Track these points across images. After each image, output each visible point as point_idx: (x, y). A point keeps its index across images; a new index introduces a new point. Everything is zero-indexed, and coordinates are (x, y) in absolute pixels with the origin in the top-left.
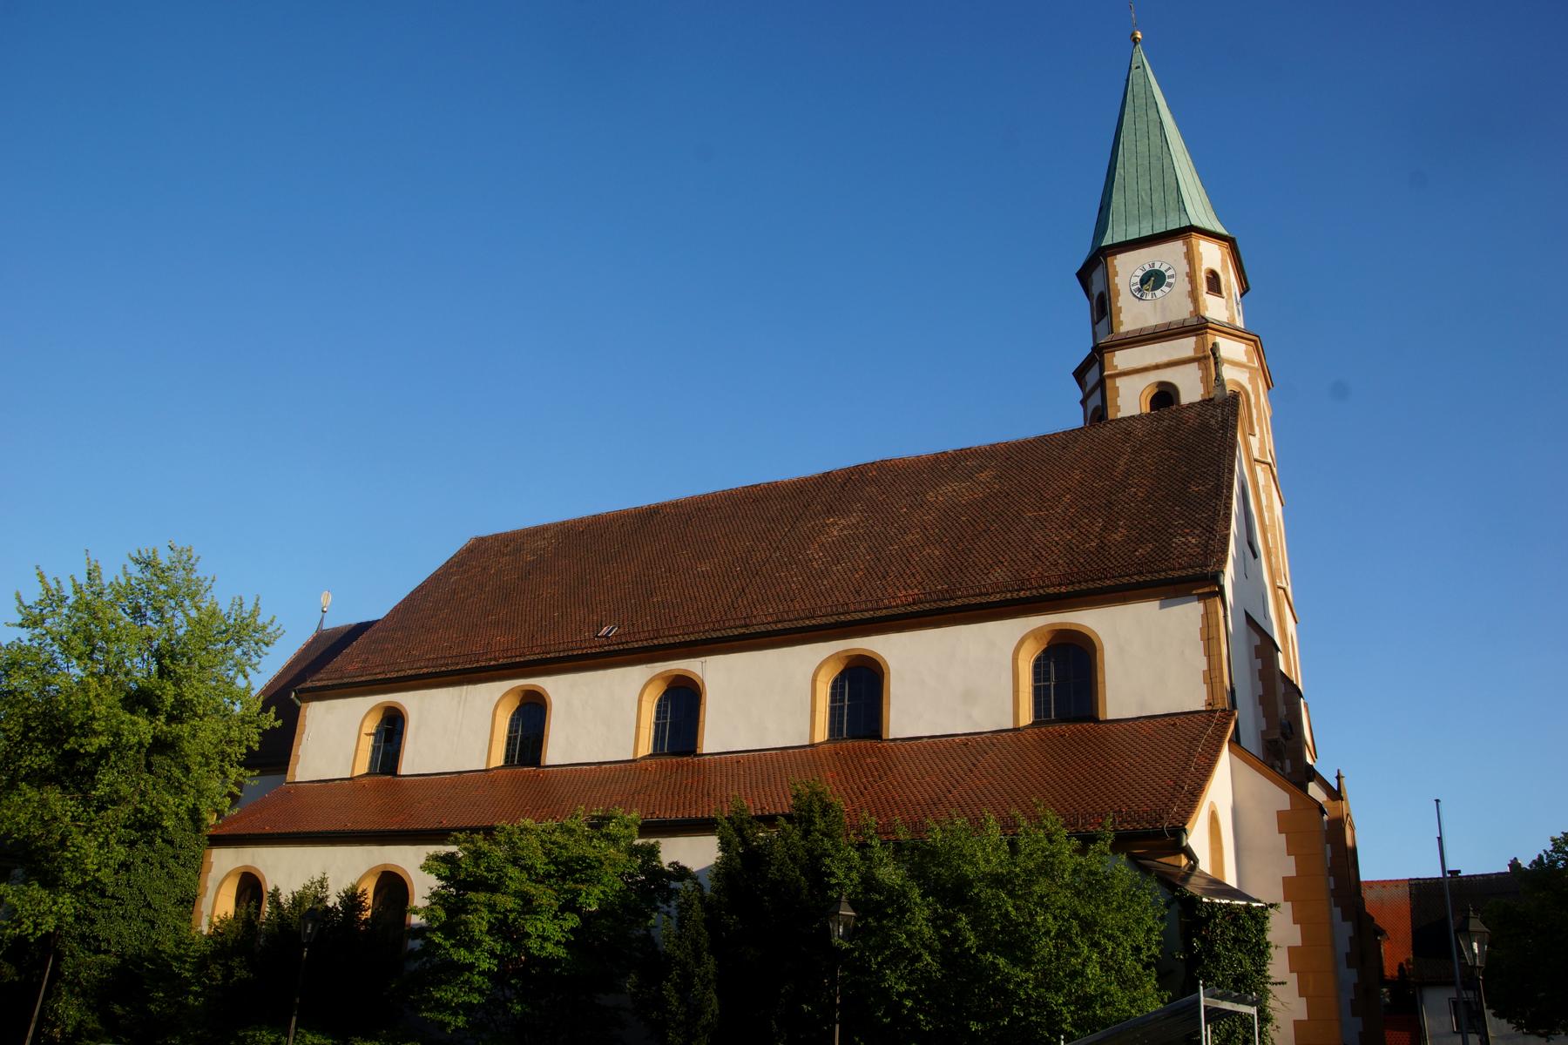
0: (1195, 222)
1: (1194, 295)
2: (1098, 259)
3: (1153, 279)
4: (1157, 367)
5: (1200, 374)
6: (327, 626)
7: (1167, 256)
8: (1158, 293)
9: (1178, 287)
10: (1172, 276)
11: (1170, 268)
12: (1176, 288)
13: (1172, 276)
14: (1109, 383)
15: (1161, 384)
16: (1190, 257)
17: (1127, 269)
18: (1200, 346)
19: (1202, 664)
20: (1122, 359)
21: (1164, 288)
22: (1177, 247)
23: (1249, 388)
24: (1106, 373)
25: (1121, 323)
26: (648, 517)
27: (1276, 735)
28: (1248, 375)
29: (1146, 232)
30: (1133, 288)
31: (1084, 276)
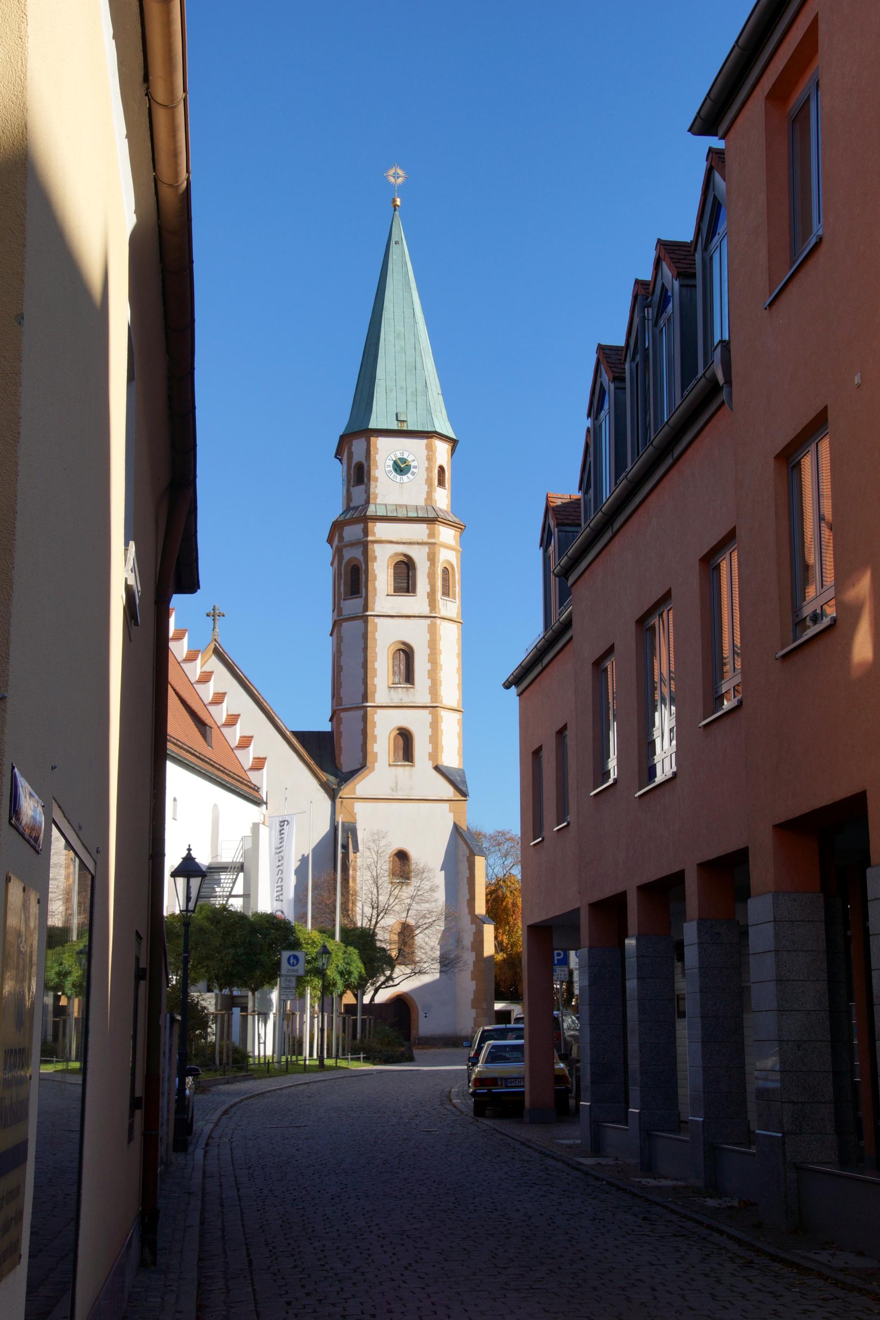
0: (439, 430)
8: (405, 477)
10: (415, 467)
11: (414, 460)
13: (415, 467)
21: (409, 475)
22: (420, 444)
30: (387, 469)
31: (345, 440)
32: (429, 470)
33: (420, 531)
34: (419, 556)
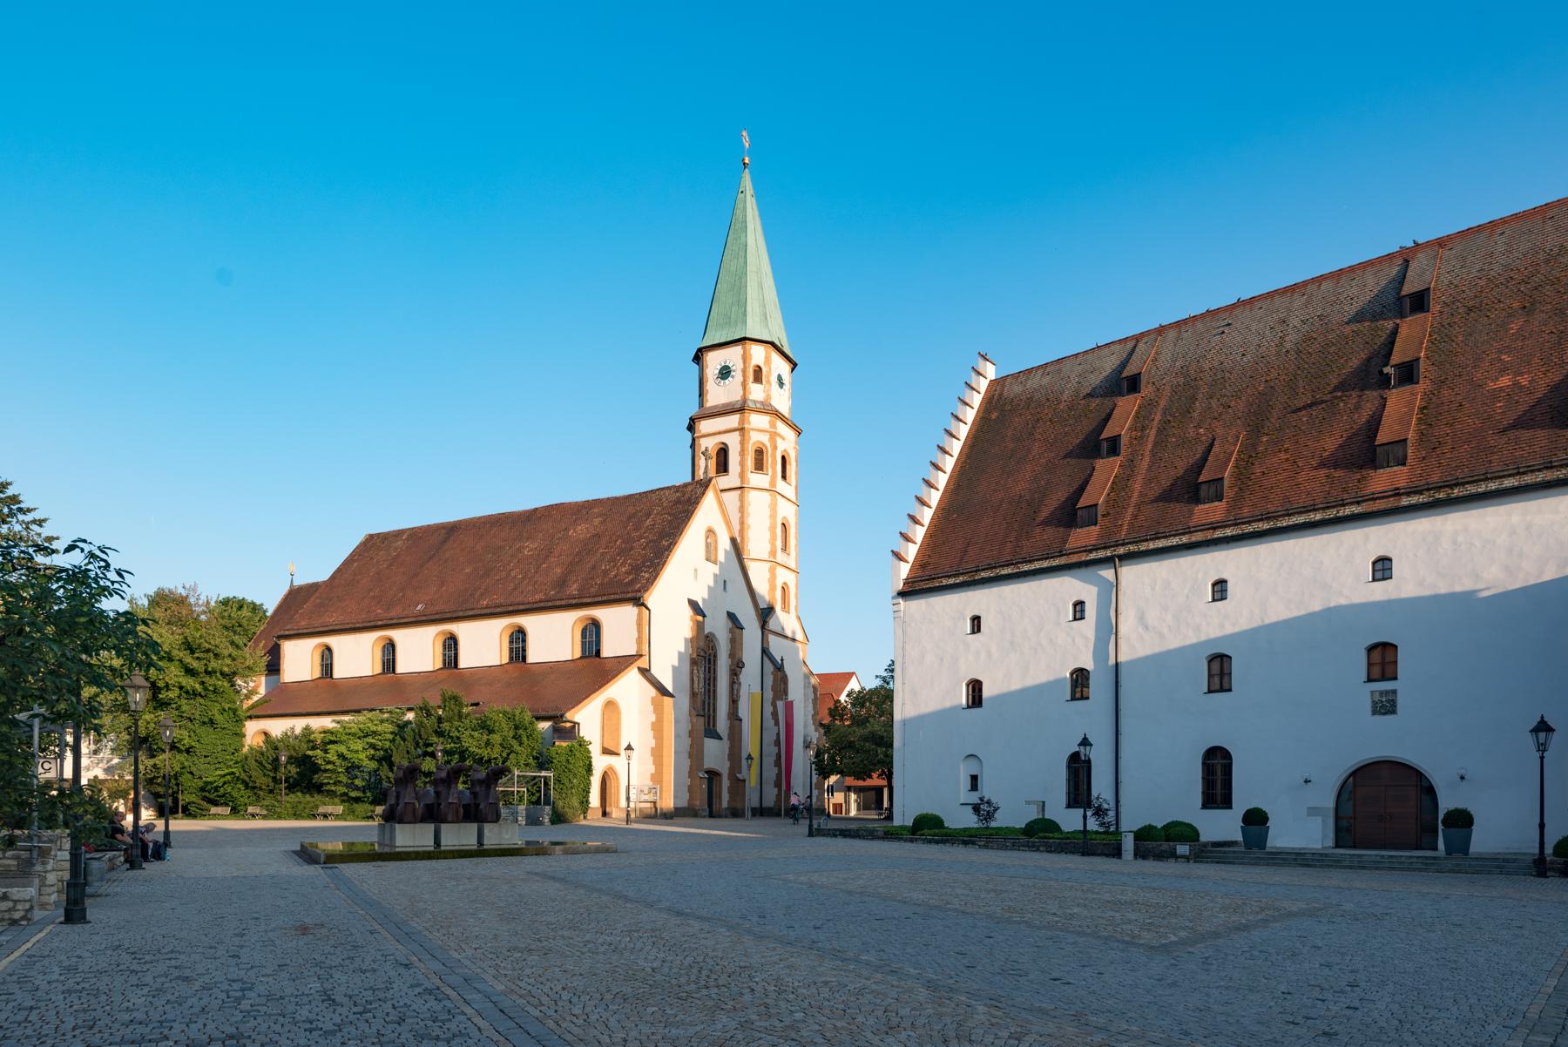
1: (744, 385)
2: (698, 358)
3: (725, 373)
4: (720, 433)
5: (739, 438)
6: (296, 583)
7: (732, 356)
8: (727, 381)
9: (737, 376)
10: (734, 371)
12: (736, 379)
13: (734, 371)
14: (696, 440)
15: (723, 443)
16: (745, 358)
17: (714, 361)
18: (742, 421)
19: (636, 635)
20: (705, 426)
21: (729, 378)
22: (737, 351)
23: (768, 445)
24: (696, 435)
25: (707, 401)
26: (451, 530)
27: (695, 656)
28: (768, 436)
29: (723, 340)
32: (744, 372)
33: (733, 421)
34: (733, 441)
